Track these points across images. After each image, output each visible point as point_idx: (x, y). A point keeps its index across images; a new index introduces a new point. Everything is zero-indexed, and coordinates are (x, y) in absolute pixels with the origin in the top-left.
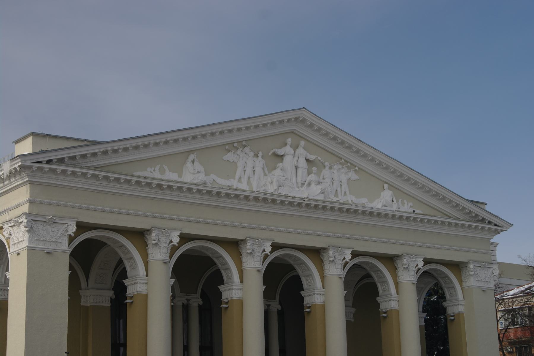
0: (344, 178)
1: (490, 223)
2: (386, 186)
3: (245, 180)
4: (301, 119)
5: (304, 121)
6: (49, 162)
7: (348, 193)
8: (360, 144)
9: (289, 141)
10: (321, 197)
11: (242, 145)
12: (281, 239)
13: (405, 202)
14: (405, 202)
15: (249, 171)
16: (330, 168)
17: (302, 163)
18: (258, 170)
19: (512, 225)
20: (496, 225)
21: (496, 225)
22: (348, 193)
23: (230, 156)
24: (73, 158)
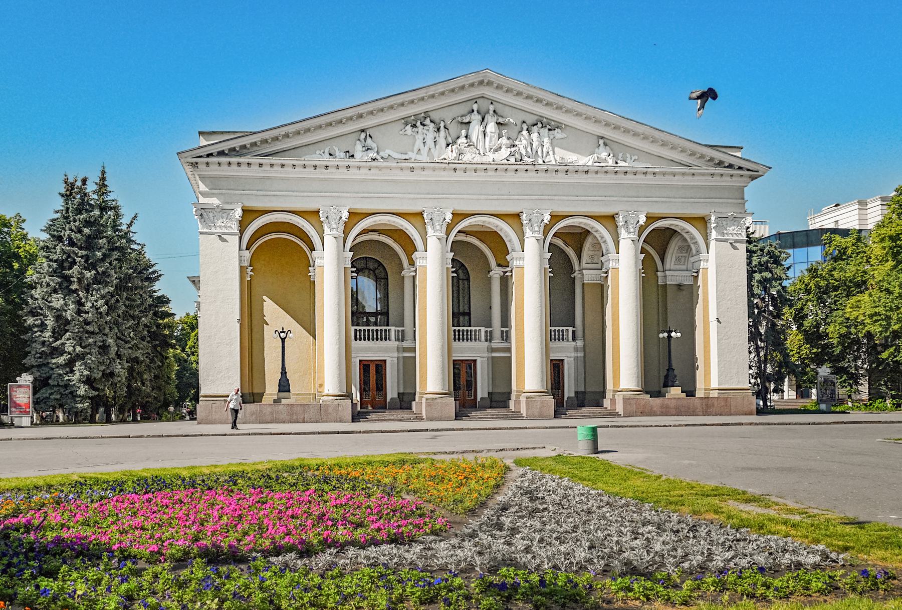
1: (740, 168)
3: (425, 151)
4: (486, 81)
5: (490, 83)
8: (559, 99)
12: (657, 210)
13: (628, 155)
14: (628, 155)
15: (430, 142)
17: (491, 127)
19: (770, 168)
20: (748, 170)
21: (748, 170)
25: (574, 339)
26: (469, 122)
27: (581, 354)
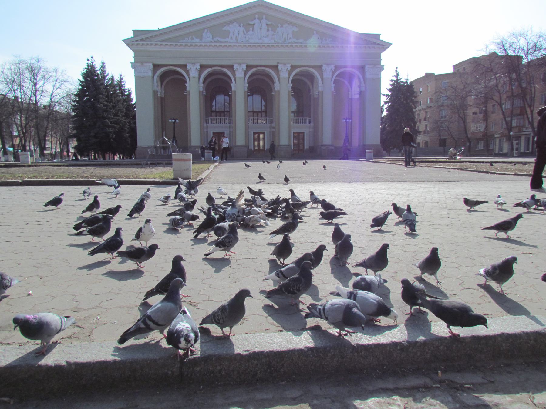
2: (315, 32)
6: (137, 41)
9: (257, 16)
10: (273, 41)
11: (231, 22)
16: (282, 26)
17: (264, 27)
18: (242, 33)
23: (226, 28)
24: (147, 38)
25: (310, 123)
26: (254, 24)
27: (312, 130)
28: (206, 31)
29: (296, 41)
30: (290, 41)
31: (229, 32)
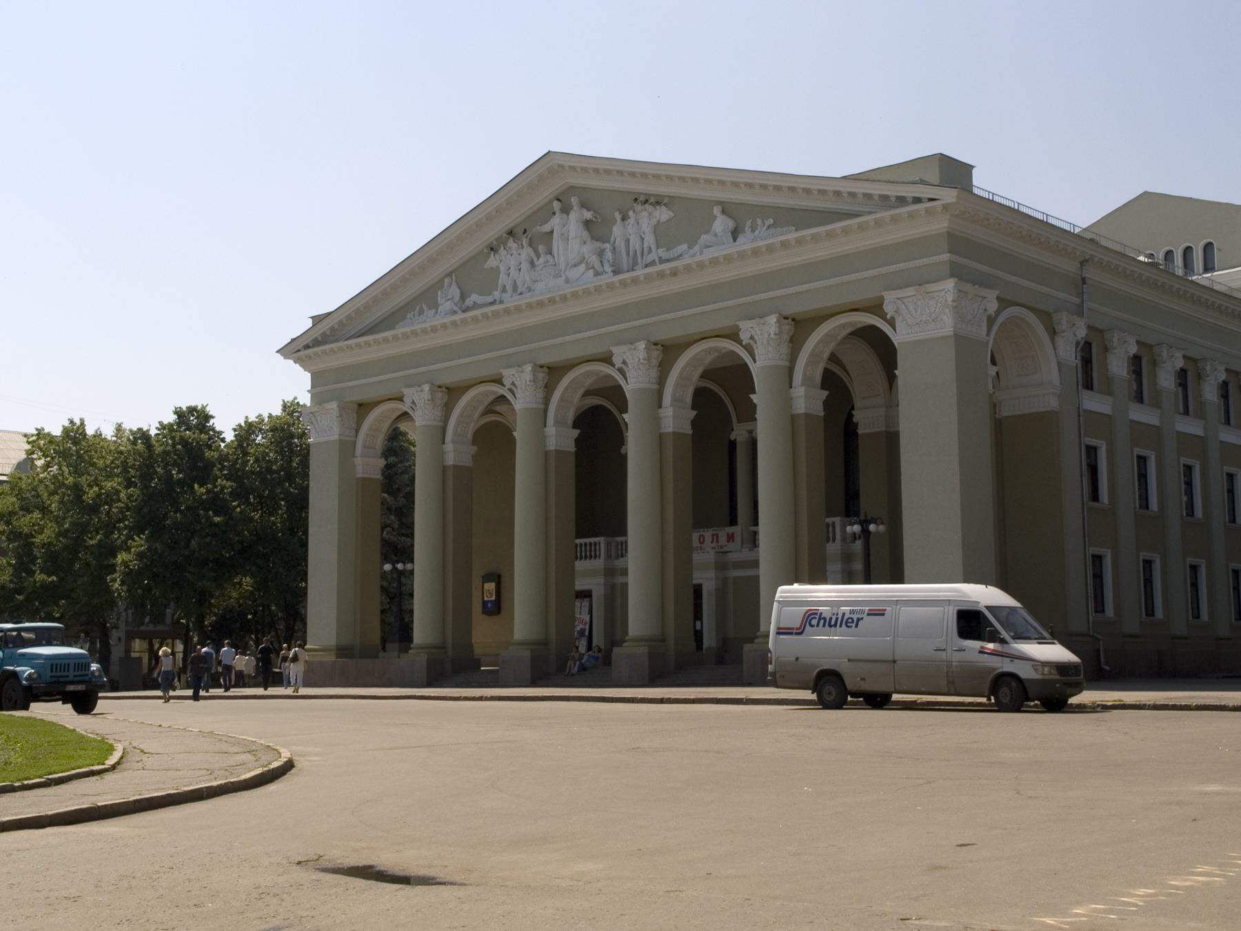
0: (646, 227)
7: (653, 247)
13: (759, 221)
14: (759, 221)
22: (653, 247)
23: (492, 261)
26: (552, 232)
28: (446, 281)
29: (665, 256)
30: (649, 259)
31: (496, 270)
